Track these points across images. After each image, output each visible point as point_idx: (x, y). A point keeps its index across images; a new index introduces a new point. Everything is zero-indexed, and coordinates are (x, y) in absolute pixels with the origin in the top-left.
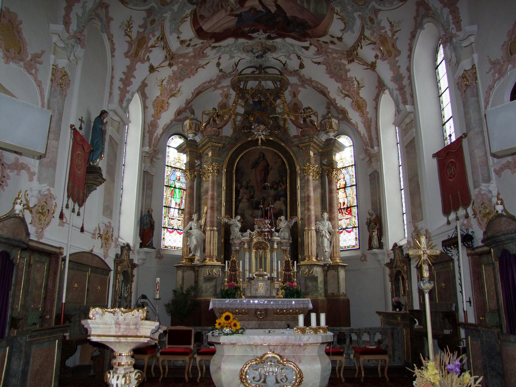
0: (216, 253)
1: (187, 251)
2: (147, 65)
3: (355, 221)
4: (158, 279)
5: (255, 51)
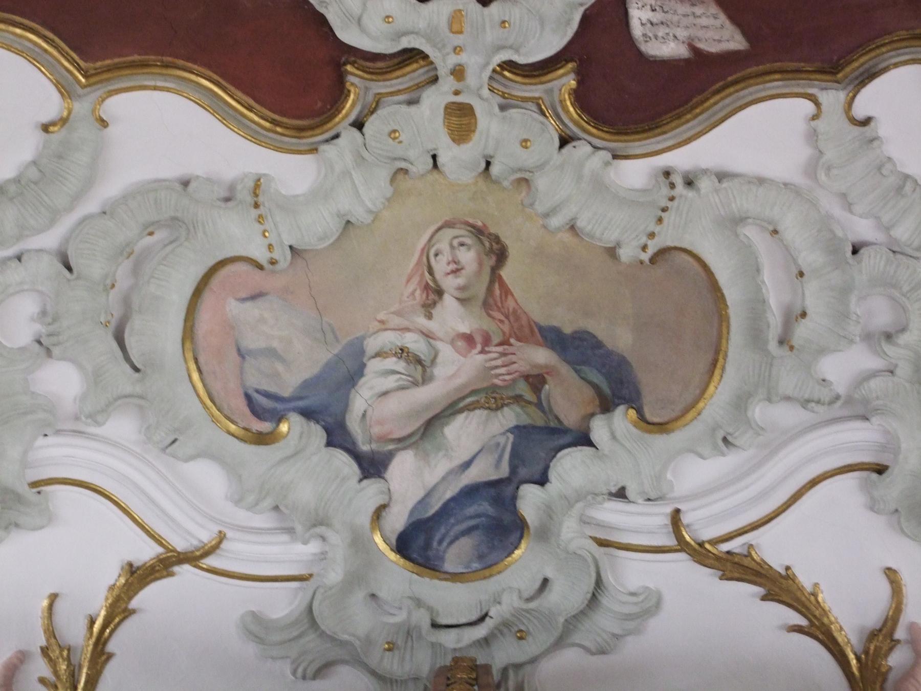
5: (379, 402)
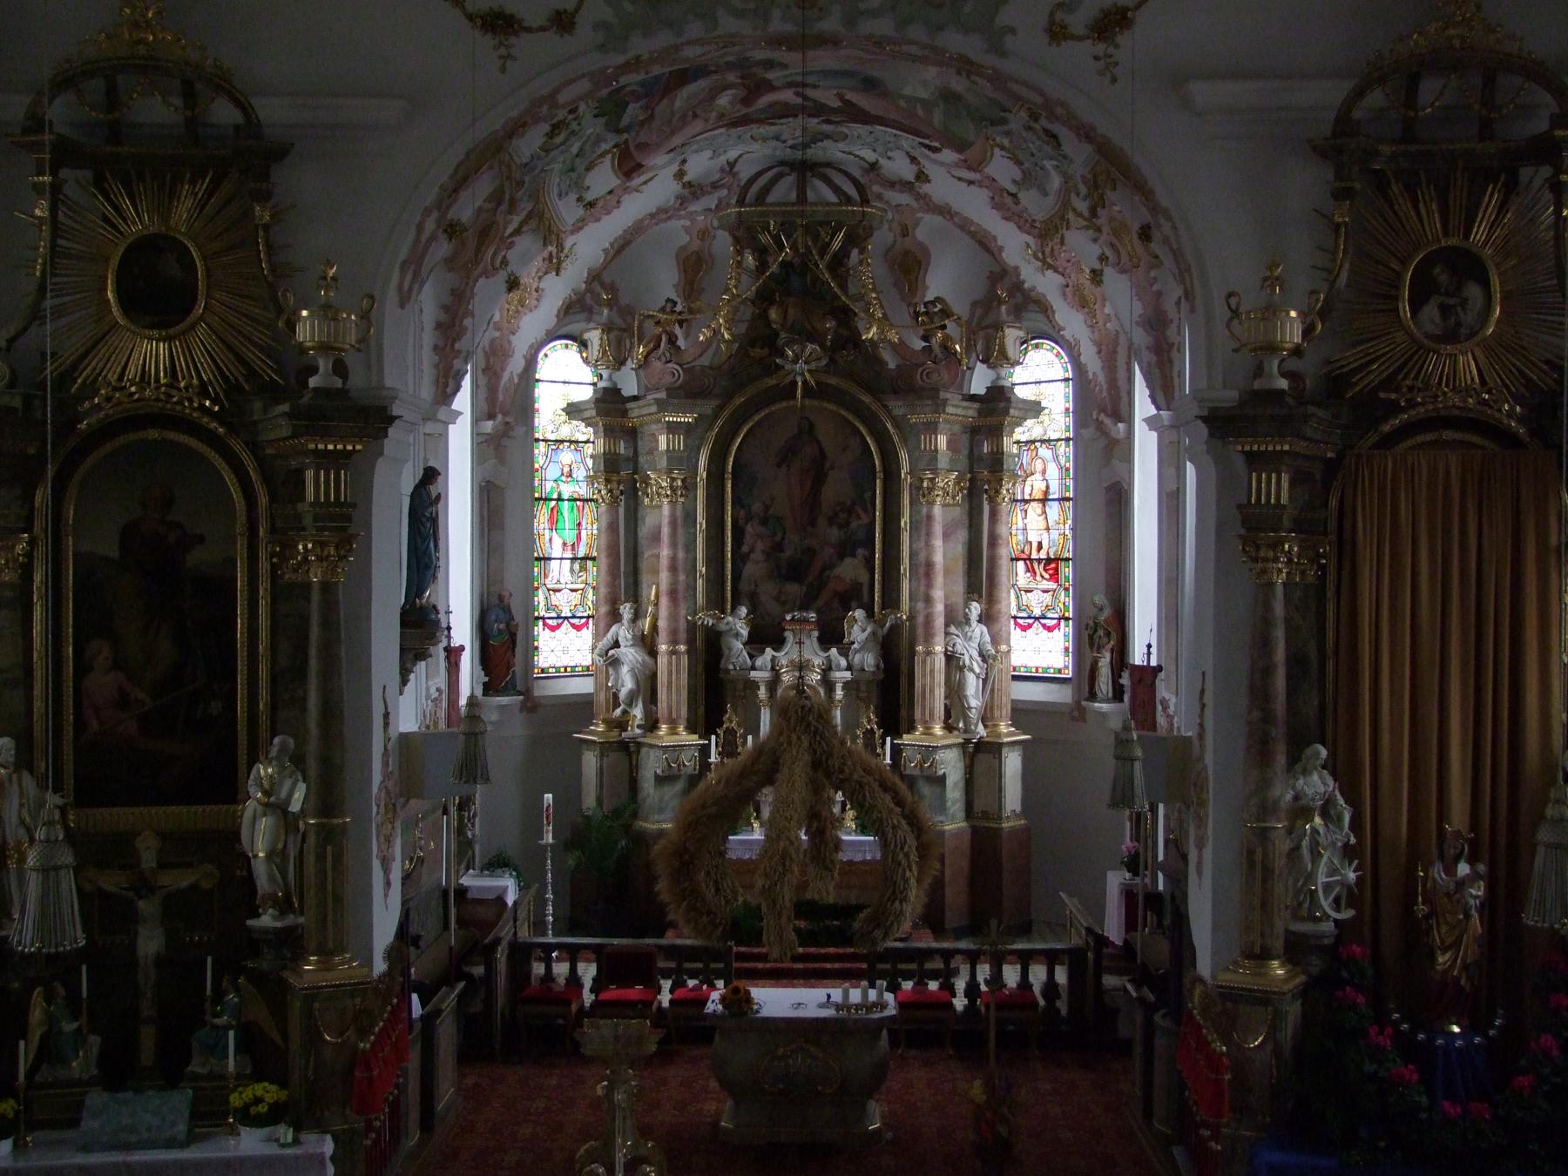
0: (684, 712)
1: (607, 701)
2: (502, 276)
3: (1066, 600)
4: (549, 797)
5: (784, 137)
